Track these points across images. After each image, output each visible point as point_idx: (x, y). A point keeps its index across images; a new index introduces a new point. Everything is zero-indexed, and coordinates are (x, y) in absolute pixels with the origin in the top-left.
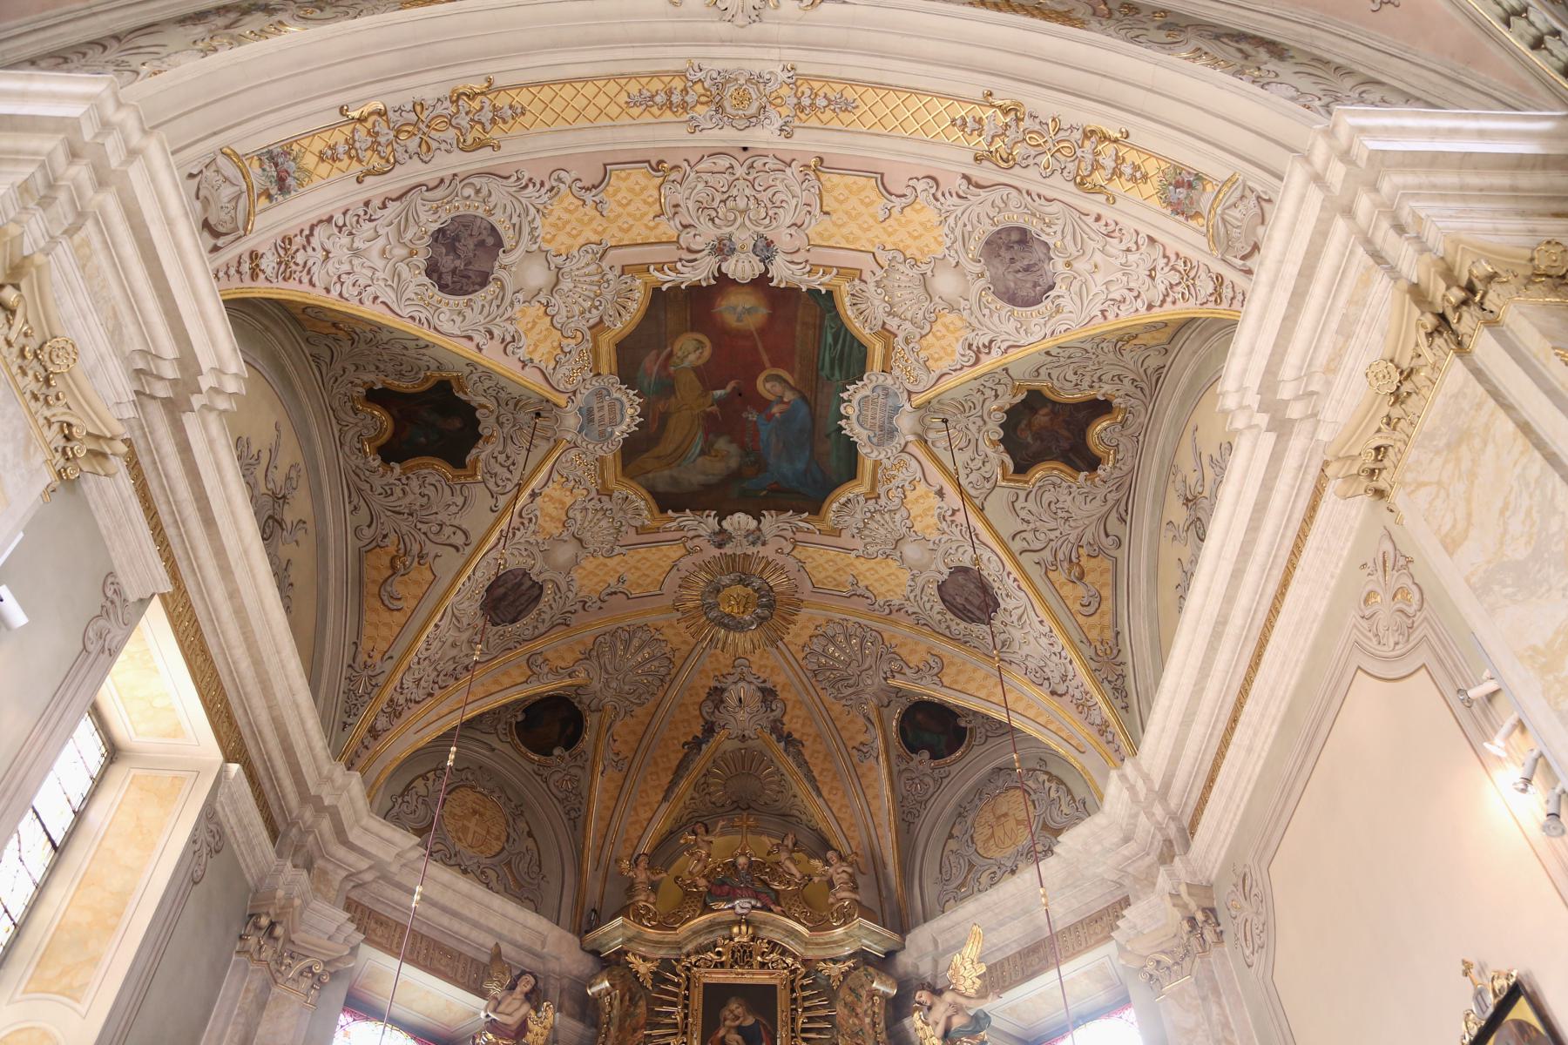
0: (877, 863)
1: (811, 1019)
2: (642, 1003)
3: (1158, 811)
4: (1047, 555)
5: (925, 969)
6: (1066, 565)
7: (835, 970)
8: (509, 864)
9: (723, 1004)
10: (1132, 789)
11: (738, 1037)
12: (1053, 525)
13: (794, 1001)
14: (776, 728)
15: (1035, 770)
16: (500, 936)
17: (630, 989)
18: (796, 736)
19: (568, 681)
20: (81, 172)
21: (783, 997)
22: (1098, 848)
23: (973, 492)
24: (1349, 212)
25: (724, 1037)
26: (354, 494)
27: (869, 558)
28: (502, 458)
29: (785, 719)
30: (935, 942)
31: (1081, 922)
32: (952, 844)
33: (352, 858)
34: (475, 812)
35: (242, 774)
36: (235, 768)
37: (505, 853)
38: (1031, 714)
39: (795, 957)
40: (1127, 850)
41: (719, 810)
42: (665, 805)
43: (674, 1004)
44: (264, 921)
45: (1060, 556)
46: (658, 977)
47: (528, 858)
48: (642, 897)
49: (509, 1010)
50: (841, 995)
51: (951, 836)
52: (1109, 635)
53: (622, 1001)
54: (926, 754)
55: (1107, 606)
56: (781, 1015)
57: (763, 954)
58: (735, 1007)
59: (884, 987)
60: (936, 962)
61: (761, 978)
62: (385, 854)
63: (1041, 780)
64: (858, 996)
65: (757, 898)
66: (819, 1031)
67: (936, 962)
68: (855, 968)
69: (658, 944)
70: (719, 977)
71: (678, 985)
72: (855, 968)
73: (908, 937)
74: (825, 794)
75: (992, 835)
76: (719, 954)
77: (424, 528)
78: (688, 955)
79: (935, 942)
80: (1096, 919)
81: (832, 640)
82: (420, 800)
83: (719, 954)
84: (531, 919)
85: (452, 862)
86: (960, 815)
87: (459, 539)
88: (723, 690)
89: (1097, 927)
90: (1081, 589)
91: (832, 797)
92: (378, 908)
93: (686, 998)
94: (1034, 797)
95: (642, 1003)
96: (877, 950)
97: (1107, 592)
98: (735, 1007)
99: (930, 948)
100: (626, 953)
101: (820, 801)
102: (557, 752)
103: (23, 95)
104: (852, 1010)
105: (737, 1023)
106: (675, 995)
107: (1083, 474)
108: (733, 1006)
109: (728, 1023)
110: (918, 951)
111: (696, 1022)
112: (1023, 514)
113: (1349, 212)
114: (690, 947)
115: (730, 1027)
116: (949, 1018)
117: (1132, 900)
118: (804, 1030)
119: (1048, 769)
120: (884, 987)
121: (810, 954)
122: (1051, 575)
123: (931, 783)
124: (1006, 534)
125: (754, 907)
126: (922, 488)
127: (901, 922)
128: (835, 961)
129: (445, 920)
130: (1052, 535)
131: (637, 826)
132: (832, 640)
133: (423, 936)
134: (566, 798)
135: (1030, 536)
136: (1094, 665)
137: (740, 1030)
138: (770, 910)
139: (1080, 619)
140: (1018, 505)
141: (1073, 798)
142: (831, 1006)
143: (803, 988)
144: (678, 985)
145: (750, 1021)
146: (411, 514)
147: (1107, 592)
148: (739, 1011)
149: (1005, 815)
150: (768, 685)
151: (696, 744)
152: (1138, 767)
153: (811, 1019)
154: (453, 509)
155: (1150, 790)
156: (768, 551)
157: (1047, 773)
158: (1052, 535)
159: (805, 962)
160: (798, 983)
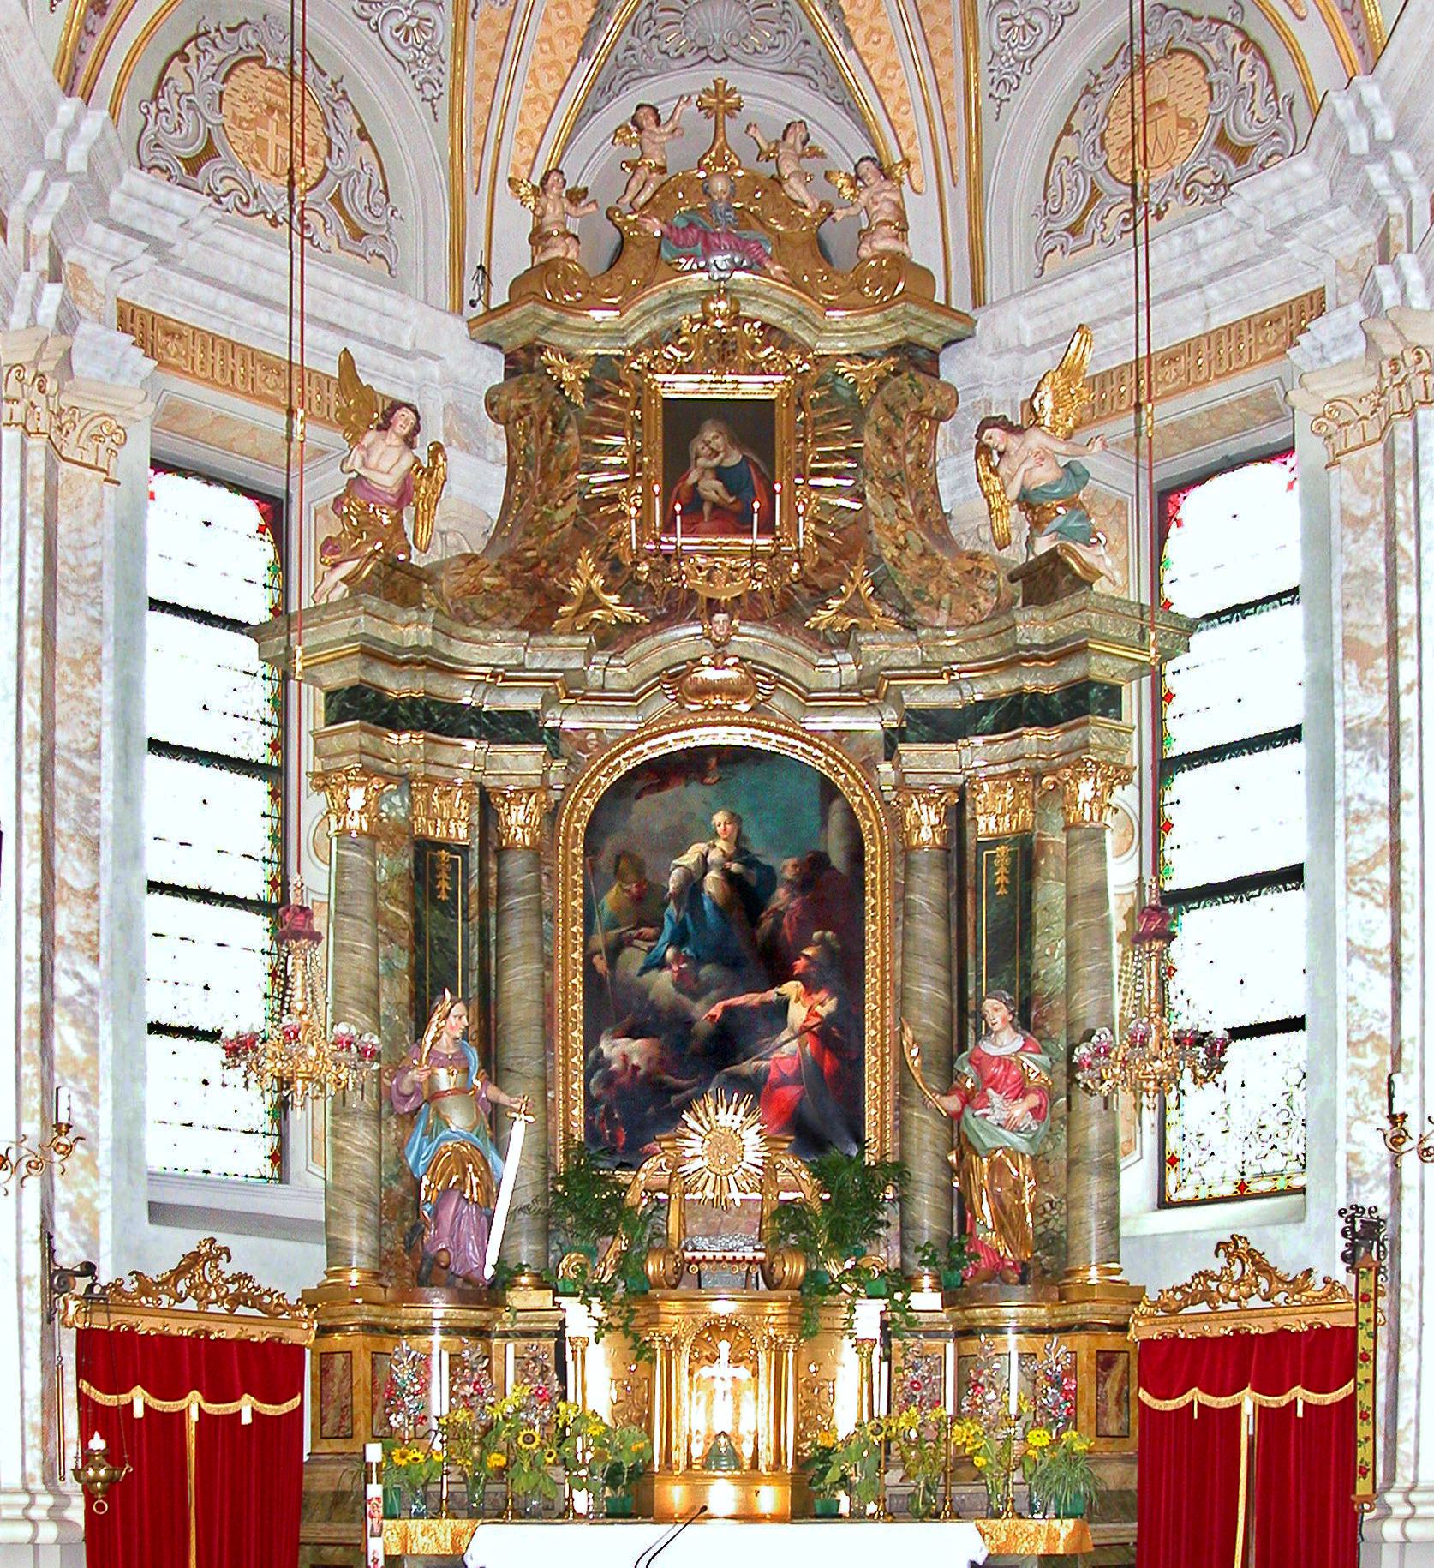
1: (825, 457)
8: (337, 200)
9: (695, 432)
11: (718, 484)
15: (1223, 22)
16: (348, 333)
17: (552, 411)
25: (696, 484)
31: (1248, 320)
32: (1069, 146)
34: (271, 108)
37: (330, 177)
39: (804, 350)
41: (677, 64)
42: (584, 66)
46: (594, 390)
47: (365, 178)
50: (872, 415)
51: (1068, 130)
53: (541, 431)
58: (711, 436)
61: (752, 388)
63: (1229, 44)
68: (896, 373)
70: (683, 386)
71: (622, 401)
72: (896, 373)
74: (858, 39)
78: (637, 350)
80: (1270, 319)
82: (184, 103)
83: (682, 348)
85: (252, 210)
86: (1088, 90)
89: (1271, 333)
91: (870, 48)
94: (1214, 76)
98: (711, 436)
100: (541, 350)
105: (716, 461)
106: (620, 417)
109: (701, 461)
114: (639, 335)
115: (705, 468)
117: (1330, 299)
119: (1245, 25)
123: (1044, 25)
128: (866, 358)
131: (538, 107)
133: (234, 344)
134: (415, 61)
137: (720, 473)
141: (1275, 91)
142: (856, 435)
144: (622, 401)
145: (734, 458)
148: (718, 443)
149: (1162, 104)
153: (825, 457)
157: (1241, 31)
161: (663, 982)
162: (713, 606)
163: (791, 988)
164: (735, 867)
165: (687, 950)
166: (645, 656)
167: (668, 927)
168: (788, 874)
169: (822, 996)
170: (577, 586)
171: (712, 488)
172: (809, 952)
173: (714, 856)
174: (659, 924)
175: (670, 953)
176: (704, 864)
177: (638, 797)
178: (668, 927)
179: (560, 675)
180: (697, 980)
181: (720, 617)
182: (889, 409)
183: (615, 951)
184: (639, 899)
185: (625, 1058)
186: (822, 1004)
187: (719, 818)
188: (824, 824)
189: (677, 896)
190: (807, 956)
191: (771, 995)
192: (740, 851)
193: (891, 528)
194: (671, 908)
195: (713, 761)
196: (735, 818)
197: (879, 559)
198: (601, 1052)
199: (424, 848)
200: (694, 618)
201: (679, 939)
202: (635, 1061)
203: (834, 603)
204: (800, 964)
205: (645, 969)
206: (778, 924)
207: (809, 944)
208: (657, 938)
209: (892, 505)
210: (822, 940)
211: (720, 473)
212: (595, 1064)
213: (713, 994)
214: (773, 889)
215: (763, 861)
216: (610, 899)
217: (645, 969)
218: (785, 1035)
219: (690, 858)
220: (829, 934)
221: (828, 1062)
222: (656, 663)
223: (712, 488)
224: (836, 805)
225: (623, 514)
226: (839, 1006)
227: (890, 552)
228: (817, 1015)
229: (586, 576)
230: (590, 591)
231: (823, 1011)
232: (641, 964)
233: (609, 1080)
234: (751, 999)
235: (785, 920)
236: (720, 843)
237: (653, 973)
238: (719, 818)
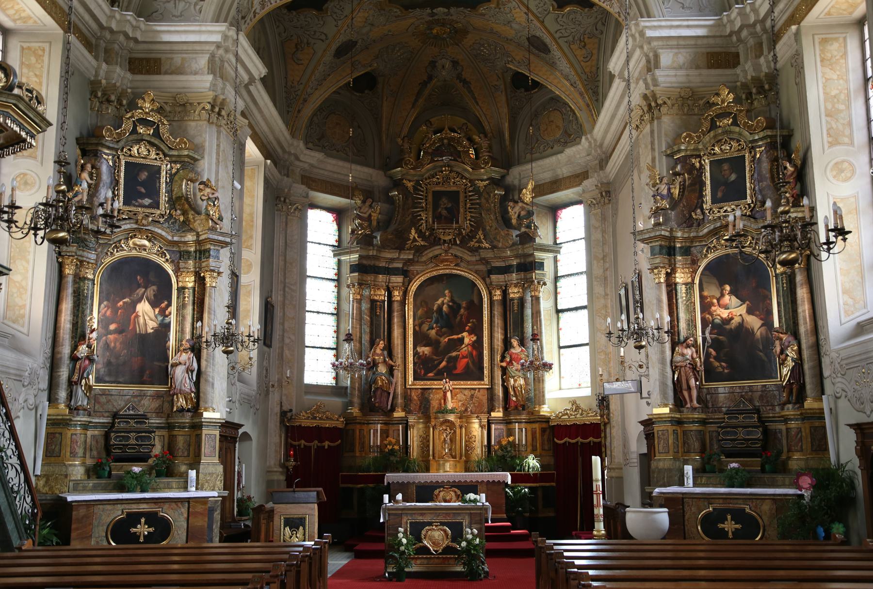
0: (501, 134)
2: (410, 199)
3: (599, 151)
4: (570, 38)
5: (516, 182)
6: (578, 42)
7: (481, 184)
10: (590, 142)
12: (573, 26)
13: (466, 197)
14: (459, 77)
18: (468, 80)
19: (369, 69)
20: (221, 52)
21: (462, 196)
22: (578, 156)
23: (539, 15)
24: (641, 47)
26: (277, 23)
27: (497, 24)
28: (338, 7)
29: (463, 73)
30: (520, 174)
33: (301, 164)
35: (272, 165)
36: (269, 161)
38: (563, 89)
39: (466, 179)
40: (588, 158)
43: (422, 199)
44: (282, 199)
45: (576, 38)
48: (407, 156)
49: (365, 211)
52: (594, 69)
54: (523, 90)
55: (595, 57)
56: (461, 204)
57: (454, 178)
58: (444, 200)
59: (499, 192)
60: (520, 180)
62: (313, 162)
64: (490, 196)
65: (451, 156)
66: (475, 209)
67: (520, 180)
69: (414, 176)
70: (438, 189)
73: (510, 170)
75: (546, 129)
76: (438, 178)
77: (308, 33)
79: (520, 174)
81: (483, 45)
84: (366, 170)
87: (323, 37)
88: (435, 62)
90: (584, 51)
92: (312, 176)
93: (426, 197)
95: (410, 199)
96: (497, 176)
97: (595, 52)
98: (444, 200)
99: (518, 177)
100: (403, 180)
101: (478, 107)
102: (366, 92)
103: (200, 32)
104: (487, 200)
107: (586, 9)
108: (444, 200)
110: (515, 174)
111: (430, 207)
112: (561, 23)
113: (641, 47)
114: (426, 176)
116: (520, 213)
118: (469, 208)
120: (499, 192)
121: (472, 178)
122: (572, 46)
124: (552, 31)
125: (451, 160)
126: (518, 10)
127: (507, 161)
128: (482, 180)
129: (335, 176)
130: (573, 30)
132: (483, 45)
135: (563, 31)
136: (586, 83)
137: (446, 209)
138: (457, 161)
139: (582, 63)
140: (558, 20)
142: (479, 198)
143: (470, 192)
144: (423, 192)
145: (450, 205)
146: (301, 28)
147: (595, 52)
148: (446, 201)
150: (455, 60)
151: (425, 84)
152: (592, 137)
154: (319, 26)
155: (595, 145)
156: (454, 18)
158: (573, 30)
159: (471, 181)
160: (467, 190)
161: (433, 333)
162: (445, 241)
163: (465, 334)
164: (450, 304)
165: (439, 325)
167: (434, 319)
168: (464, 305)
169: (473, 336)
170: (411, 238)
171: (444, 212)
173: (445, 301)
174: (432, 318)
175: (434, 326)
176: (443, 304)
178: (434, 319)
181: (446, 245)
182: (488, 193)
183: (420, 325)
184: (426, 312)
185: (423, 352)
187: (447, 292)
188: (473, 292)
189: (437, 311)
191: (460, 336)
192: (452, 300)
193: (488, 222)
194: (435, 314)
196: (450, 292)
197: (485, 229)
199: (373, 302)
200: (440, 245)
201: (437, 322)
202: (426, 352)
203: (475, 240)
204: (467, 328)
205: (428, 330)
206: (461, 318)
207: (469, 323)
209: (488, 216)
210: (472, 322)
211: (446, 209)
212: (416, 354)
214: (460, 309)
216: (420, 312)
217: (428, 330)
218: (463, 346)
219: (440, 301)
221: (474, 353)
222: (431, 255)
223: (444, 212)
225: (422, 219)
227: (488, 228)
229: (413, 233)
230: (414, 237)
231: (473, 339)
232: (427, 328)
233: (419, 357)
234: (455, 337)
236: (447, 298)
237: (430, 331)
238: (447, 292)
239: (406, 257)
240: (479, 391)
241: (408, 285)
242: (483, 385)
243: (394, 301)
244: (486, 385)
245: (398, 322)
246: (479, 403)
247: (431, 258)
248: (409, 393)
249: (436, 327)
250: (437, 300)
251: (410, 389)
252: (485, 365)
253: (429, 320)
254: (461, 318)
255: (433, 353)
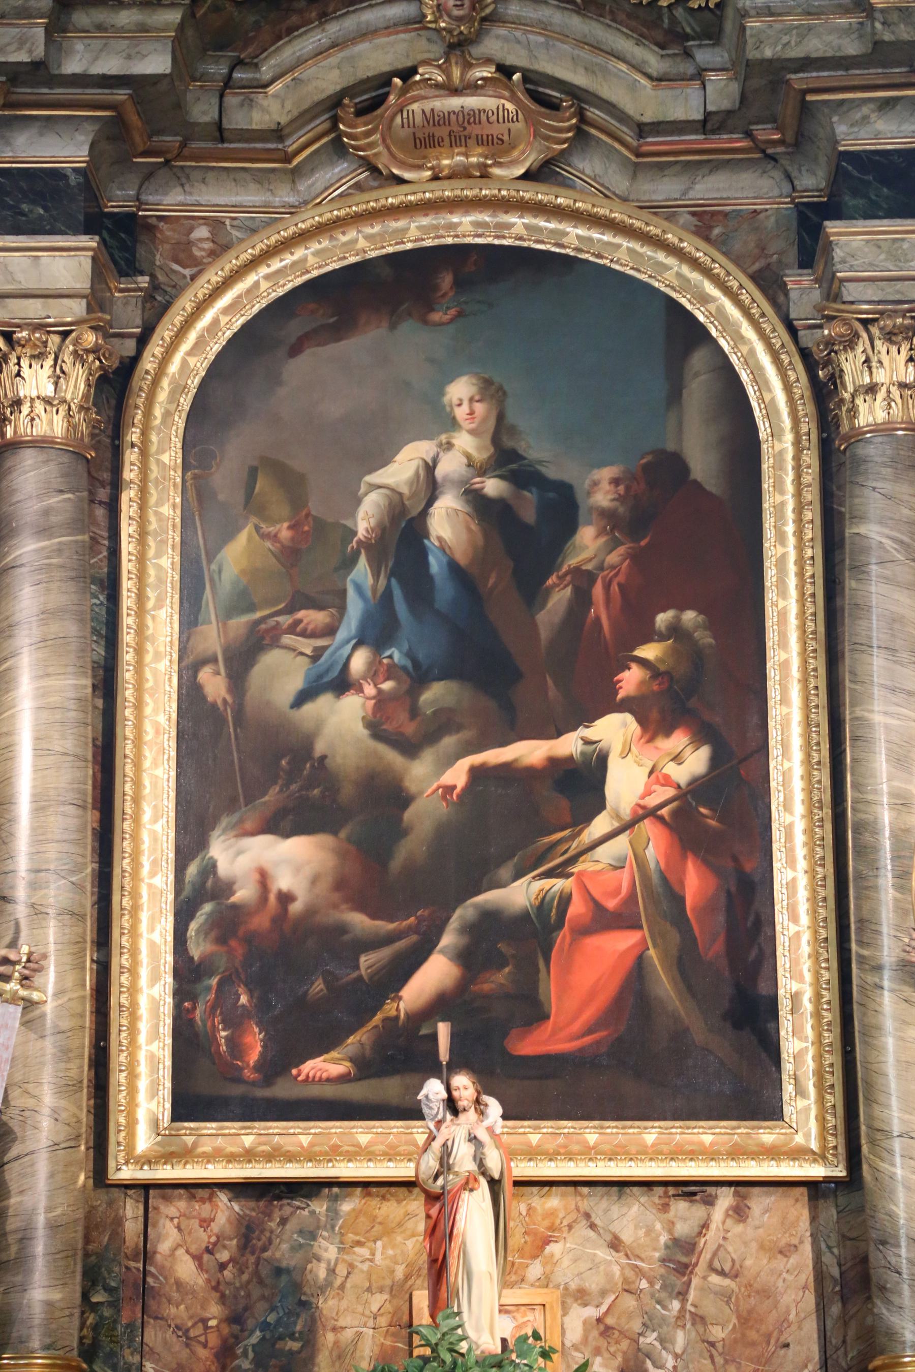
164: (492, 486)
165: (396, 655)
166: (300, 62)
168: (603, 498)
169: (679, 740)
172: (649, 652)
175: (359, 661)
177: (295, 350)
178: (355, 608)
179: (121, 95)
180: (414, 712)
185: (264, 878)
186: (677, 759)
188: (675, 395)
190: (643, 663)
194: (362, 570)
195: (446, 281)
198: (211, 868)
202: (284, 881)
205: (304, 697)
206: (582, 598)
207: (648, 635)
208: (330, 631)
210: (675, 631)
213: (449, 742)
214: (571, 528)
215: (552, 473)
217: (304, 697)
218: (600, 825)
220: (689, 616)
224: (699, 359)
226: (715, 761)
228: (667, 781)
232: (295, 683)
235: (598, 591)
236: (464, 442)
237: (324, 703)
239: (110, 65)
240: (739, 1212)
241: (143, 340)
242: (772, 1153)
243: (16, 445)
244: (799, 1154)
245: (47, 615)
246: (746, 1320)
247: (335, 102)
248: (132, 1228)
249: (373, 673)
250: (383, 459)
251: (146, 1188)
252: (786, 986)
253: (314, 618)
254: (582, 598)
255: (340, 885)
